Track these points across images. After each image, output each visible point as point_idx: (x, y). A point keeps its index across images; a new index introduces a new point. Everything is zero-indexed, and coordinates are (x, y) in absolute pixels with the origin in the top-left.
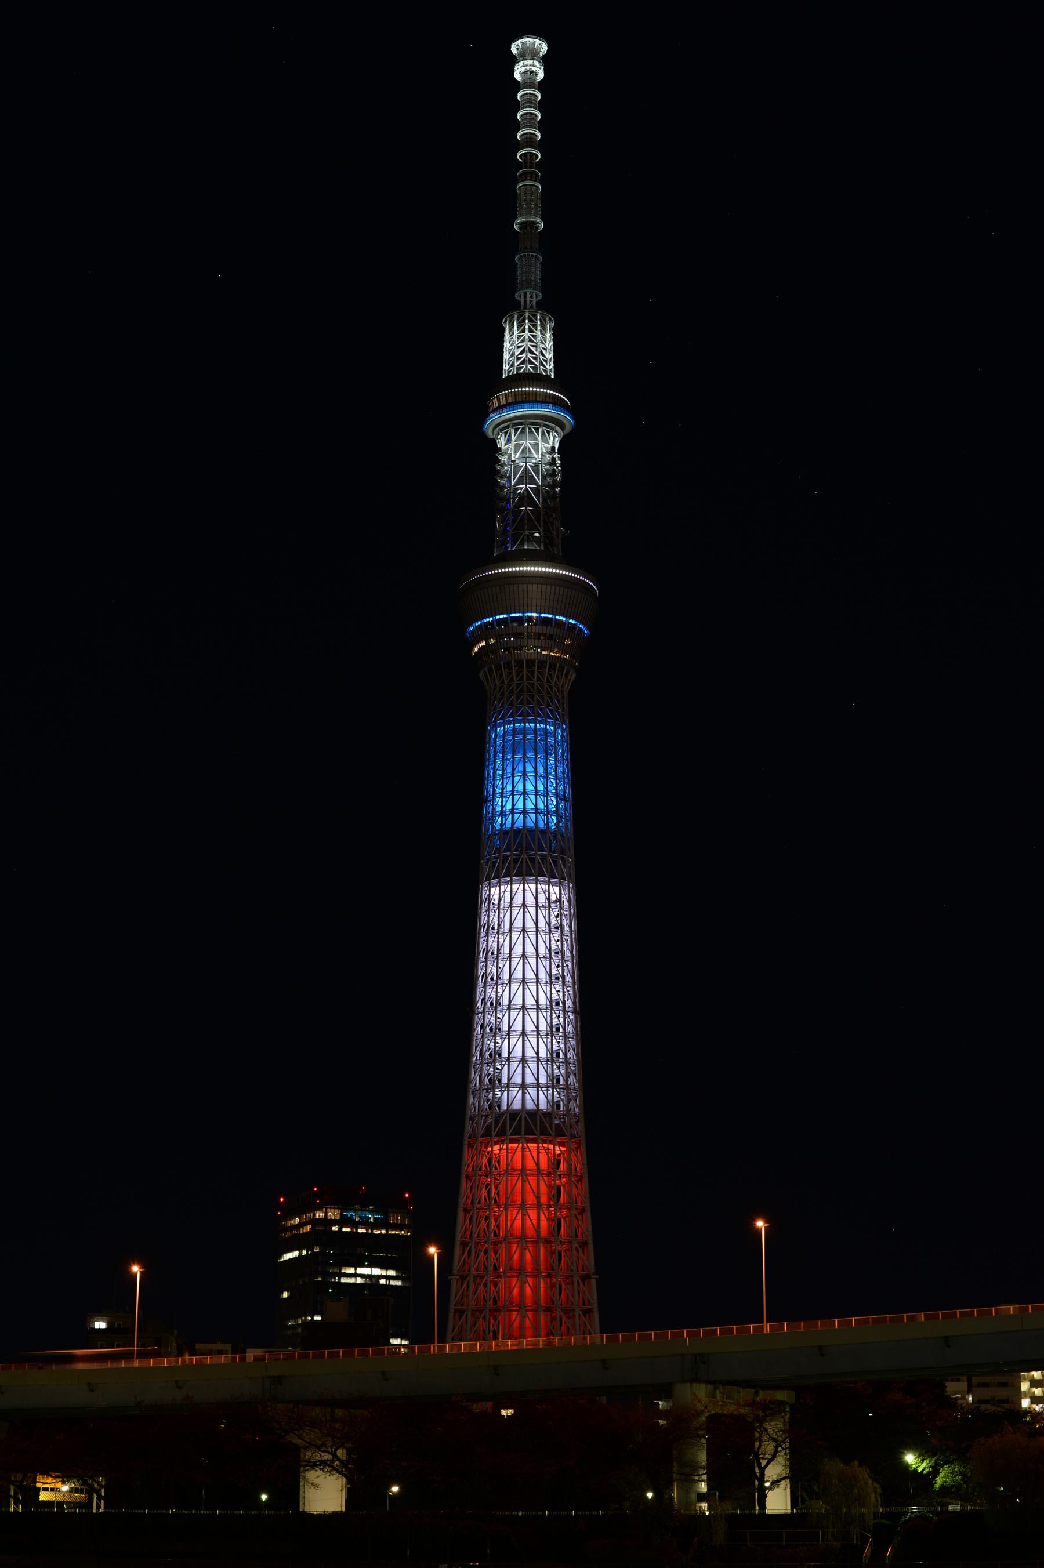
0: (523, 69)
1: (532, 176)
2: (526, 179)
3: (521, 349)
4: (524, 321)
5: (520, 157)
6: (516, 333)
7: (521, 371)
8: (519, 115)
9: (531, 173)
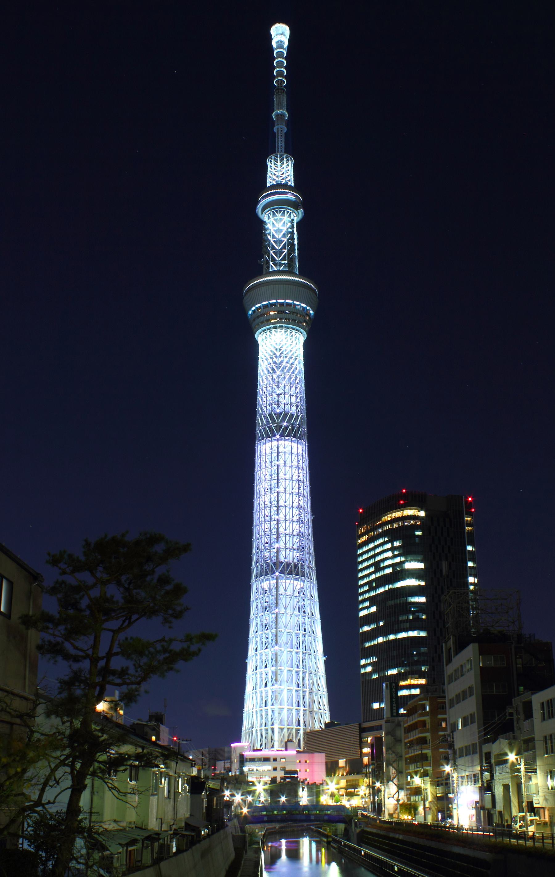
3: (282, 172)
4: (283, 159)
6: (279, 164)
7: (282, 183)
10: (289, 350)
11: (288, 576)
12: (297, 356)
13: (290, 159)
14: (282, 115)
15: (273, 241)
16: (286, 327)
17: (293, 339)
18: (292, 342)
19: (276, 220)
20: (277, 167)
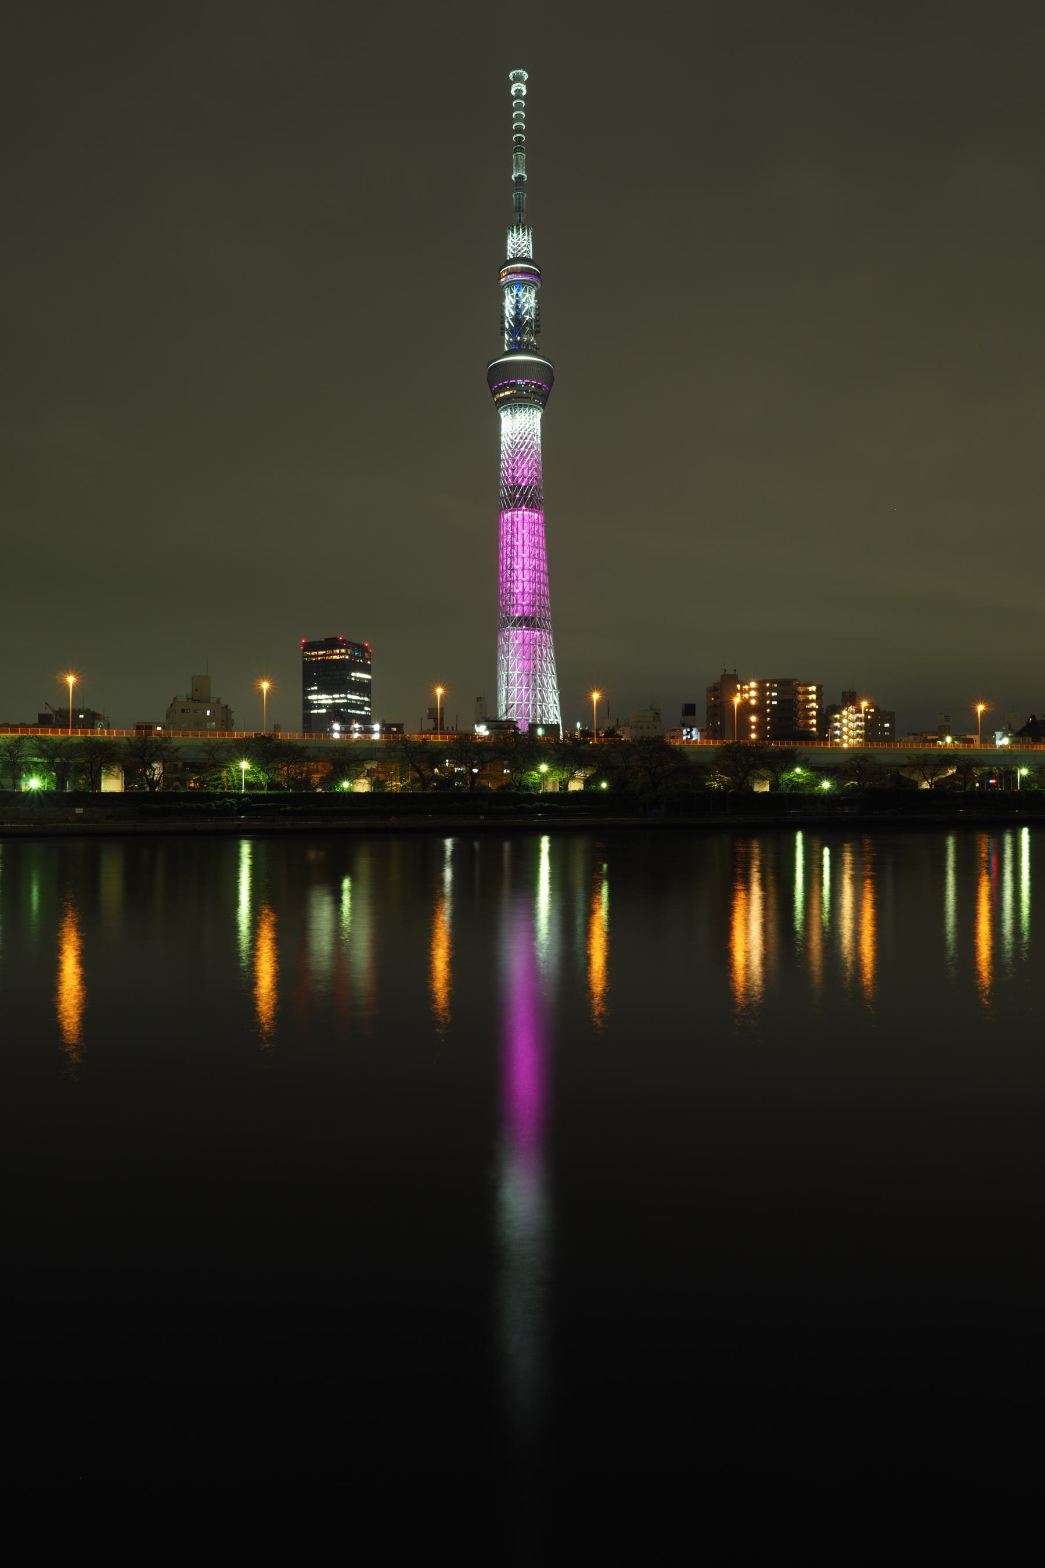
0: (516, 88)
1: (520, 150)
2: (516, 152)
4: (519, 229)
5: (515, 138)
6: (515, 235)
7: (518, 256)
8: (514, 114)
9: (520, 148)
10: (522, 426)
11: (520, 628)
12: (530, 431)
13: (526, 227)
14: (521, 177)
15: (511, 319)
16: (519, 405)
17: (527, 415)
18: (526, 418)
19: (512, 296)
20: (513, 238)
